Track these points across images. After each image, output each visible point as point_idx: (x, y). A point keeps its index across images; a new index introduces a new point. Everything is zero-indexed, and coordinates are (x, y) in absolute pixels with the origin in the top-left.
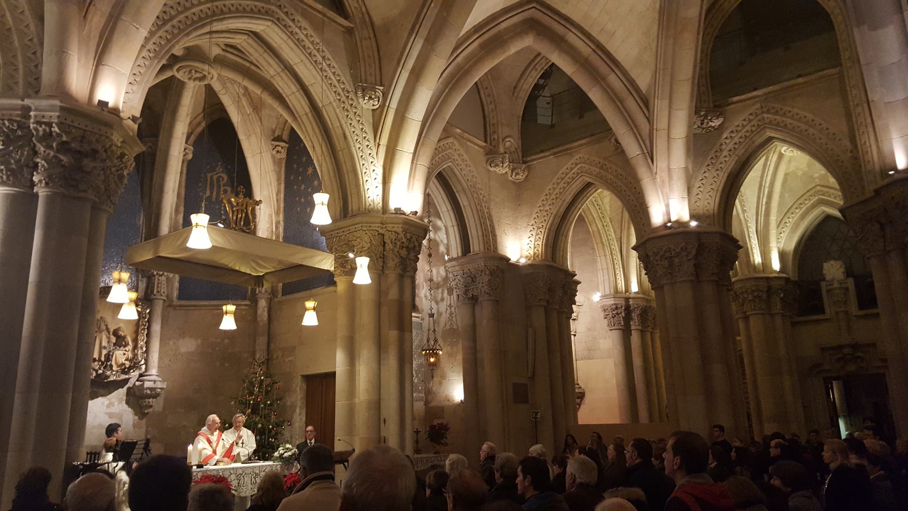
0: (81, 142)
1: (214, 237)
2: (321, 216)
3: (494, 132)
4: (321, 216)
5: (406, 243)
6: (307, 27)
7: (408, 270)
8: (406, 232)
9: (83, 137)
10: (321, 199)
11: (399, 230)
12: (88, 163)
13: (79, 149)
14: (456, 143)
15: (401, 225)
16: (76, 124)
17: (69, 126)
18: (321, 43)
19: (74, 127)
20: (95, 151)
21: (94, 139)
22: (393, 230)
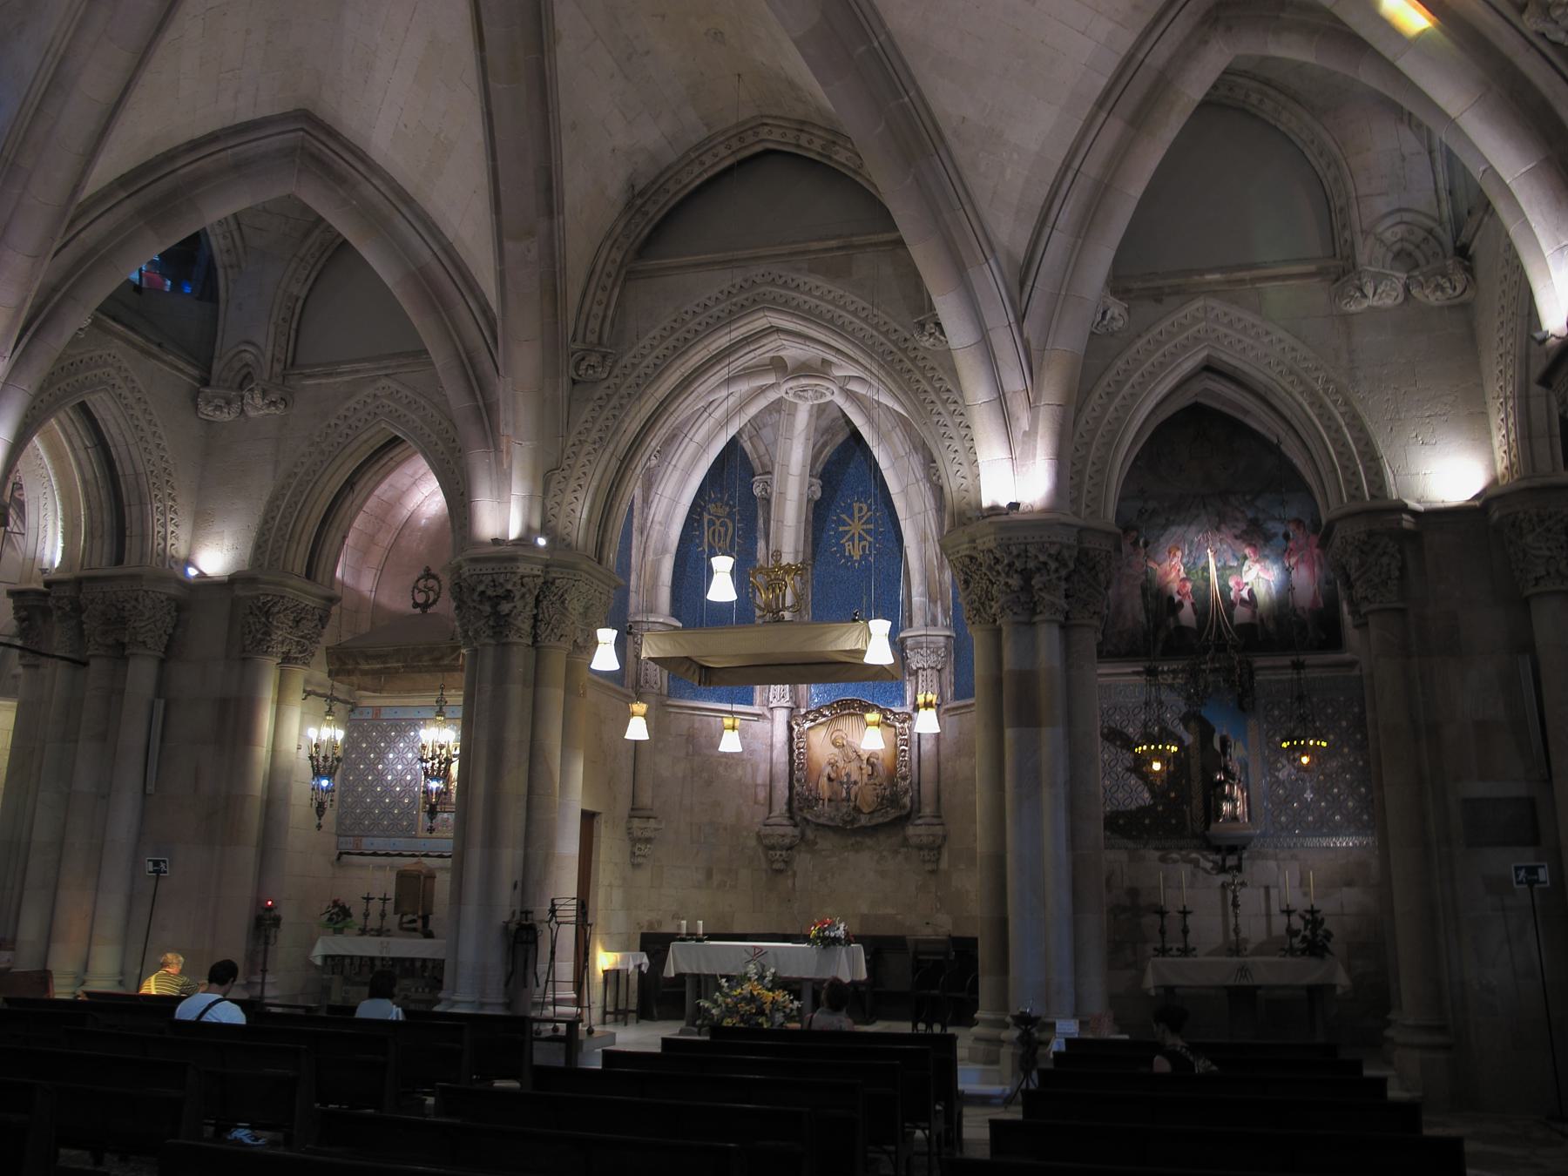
0: (495, 586)
1: (661, 645)
2: (722, 589)
3: (1344, 226)
4: (722, 589)
5: (1018, 565)
6: (819, 284)
7: (1038, 611)
8: (1008, 547)
9: (493, 581)
10: (722, 565)
11: (992, 545)
12: (505, 607)
13: (495, 594)
14: (1212, 302)
15: (992, 537)
16: (484, 571)
17: (478, 575)
18: (847, 294)
19: (483, 575)
20: (509, 591)
21: (501, 581)
22: (985, 547)
